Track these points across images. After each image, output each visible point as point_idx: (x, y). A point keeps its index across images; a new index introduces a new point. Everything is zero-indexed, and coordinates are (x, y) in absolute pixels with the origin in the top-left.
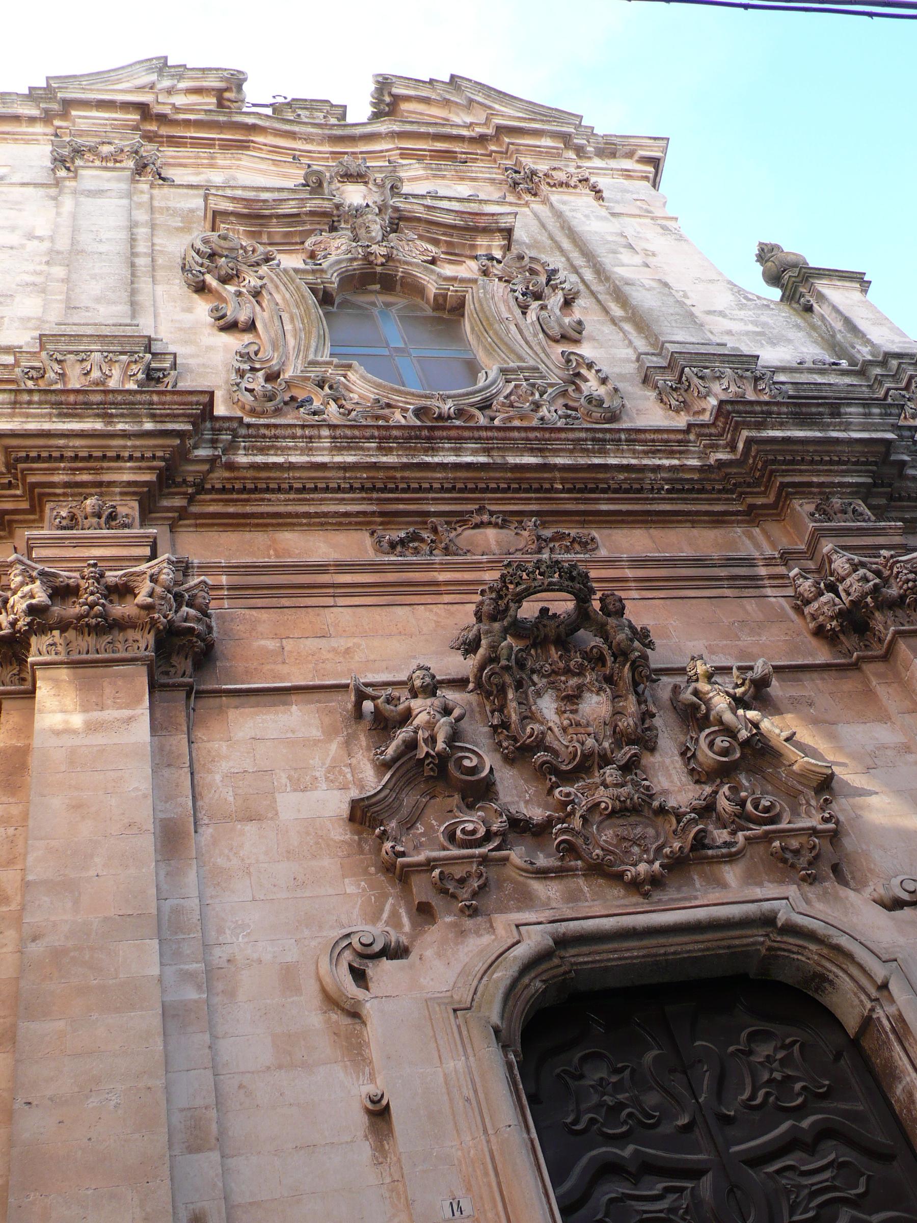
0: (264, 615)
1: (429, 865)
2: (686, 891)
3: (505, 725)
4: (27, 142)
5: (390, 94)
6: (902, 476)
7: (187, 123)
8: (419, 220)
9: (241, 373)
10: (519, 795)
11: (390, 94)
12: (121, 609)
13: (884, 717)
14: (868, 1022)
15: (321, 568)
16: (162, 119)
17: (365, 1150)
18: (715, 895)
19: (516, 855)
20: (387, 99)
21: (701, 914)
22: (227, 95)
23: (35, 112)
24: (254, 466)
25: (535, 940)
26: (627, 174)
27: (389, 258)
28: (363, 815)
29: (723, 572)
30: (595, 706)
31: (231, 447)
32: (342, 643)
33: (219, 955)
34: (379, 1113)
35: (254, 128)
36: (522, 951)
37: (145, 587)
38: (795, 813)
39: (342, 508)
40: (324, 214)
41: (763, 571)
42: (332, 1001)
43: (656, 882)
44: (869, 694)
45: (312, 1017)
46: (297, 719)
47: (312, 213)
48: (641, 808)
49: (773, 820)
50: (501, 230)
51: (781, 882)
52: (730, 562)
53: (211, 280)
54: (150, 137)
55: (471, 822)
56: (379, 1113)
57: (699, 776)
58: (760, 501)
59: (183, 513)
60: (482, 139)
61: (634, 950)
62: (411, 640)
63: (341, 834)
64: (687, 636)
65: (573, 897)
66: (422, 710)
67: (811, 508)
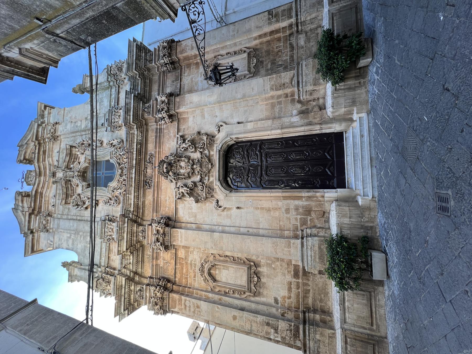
0: (162, 209)
2: (213, 160)
3: (185, 178)
4: (40, 237)
5: (23, 160)
6: (140, 94)
7: (35, 205)
8: (68, 164)
9: (110, 205)
10: (197, 178)
11: (23, 160)
12: (161, 231)
13: (188, 118)
14: (235, 141)
15: (154, 199)
16: (33, 210)
17: (241, 210)
18: (215, 156)
19: (206, 182)
20: (25, 161)
21: (217, 160)
22: (23, 195)
23: (31, 236)
24: (134, 208)
25: (218, 183)
26: (49, 113)
27: (79, 172)
28: (197, 201)
29: (158, 134)
30: (183, 164)
31: (130, 211)
32: (168, 198)
33: (215, 224)
34: (238, 208)
35: (36, 191)
36: (220, 186)
37: (158, 228)
38: (203, 140)
39: (142, 194)
40: (66, 182)
41: (159, 127)
42: (223, 211)
43: (212, 164)
44: (184, 119)
45: (225, 213)
46: (180, 206)
47: (66, 185)
48: (200, 163)
49: (204, 144)
50: (71, 148)
51: (214, 146)
52: (156, 132)
53: (84, 206)
54: (39, 212)
55: (200, 187)
56: (238, 208)
57: (195, 151)
58: (144, 123)
59: (142, 219)
60: (39, 144)
61: (221, 170)
62: (168, 190)
63: (199, 204)
64: (170, 145)
65: (213, 176)
66: (181, 190)
67: (147, 115)
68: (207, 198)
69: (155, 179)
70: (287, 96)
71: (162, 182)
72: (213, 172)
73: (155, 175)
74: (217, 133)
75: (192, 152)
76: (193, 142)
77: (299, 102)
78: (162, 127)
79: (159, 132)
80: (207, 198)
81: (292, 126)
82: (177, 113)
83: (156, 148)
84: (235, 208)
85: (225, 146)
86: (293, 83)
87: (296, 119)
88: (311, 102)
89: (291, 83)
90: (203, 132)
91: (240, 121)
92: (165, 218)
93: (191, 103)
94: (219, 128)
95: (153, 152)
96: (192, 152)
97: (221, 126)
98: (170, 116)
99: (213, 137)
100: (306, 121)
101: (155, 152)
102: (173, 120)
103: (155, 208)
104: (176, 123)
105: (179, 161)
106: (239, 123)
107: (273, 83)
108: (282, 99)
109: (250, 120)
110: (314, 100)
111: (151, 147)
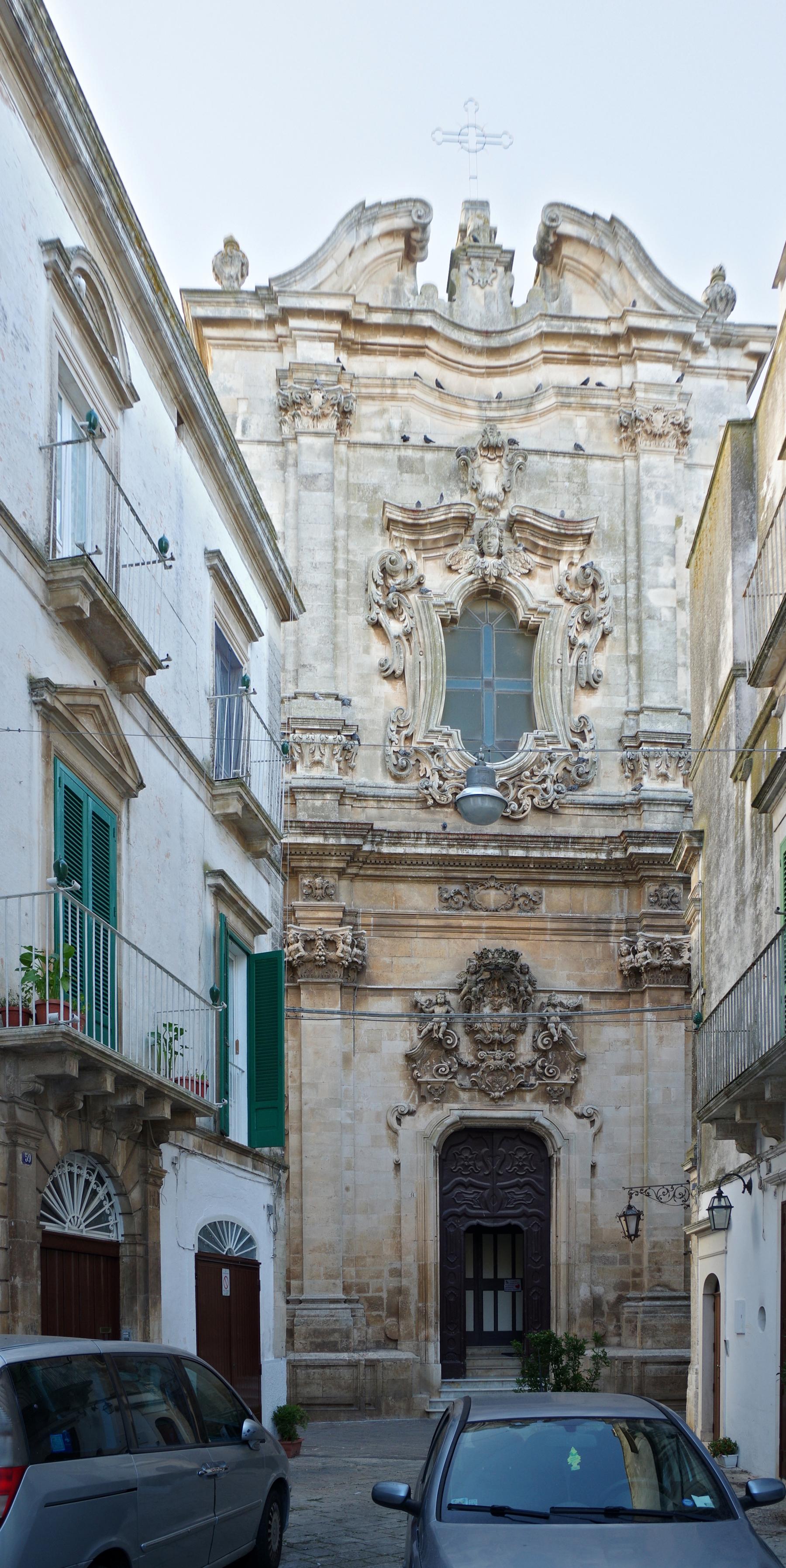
1: (428, 1083)
15: (413, 916)
17: (392, 1174)
34: (397, 1165)
42: (389, 1127)
43: (500, 1098)
45: (383, 1131)
46: (393, 1005)
51: (545, 1103)
56: (397, 1165)
57: (536, 1049)
63: (401, 1061)
65: (472, 1099)
68: (419, 1084)
69: (468, 917)
70: (637, 1274)
71: (459, 942)
72: (480, 1100)
73: (480, 918)
74: (575, 1109)
75: (535, 1041)
76: (562, 1044)
77: (620, 1299)
78: (612, 939)
79: (599, 928)
80: (419, 1084)
81: (571, 1284)
82: (643, 992)
83: (555, 919)
84: (395, 1157)
85: (542, 1133)
86: (659, 1288)
87: (584, 1292)
88: (614, 1322)
89: (658, 1285)
90: (585, 1069)
91: (599, 1169)
92: (364, 958)
93: (661, 1038)
94: (590, 1118)
95: (543, 907)
96: (535, 1041)
97: (593, 1123)
98: (635, 973)
99: (568, 1101)
100: (577, 1311)
101: (542, 919)
102: (625, 977)
103: (389, 921)
104: (616, 986)
105: (515, 1000)
106: (593, 1167)
107: (667, 1247)
108: (632, 1266)
109: (598, 1193)
110: (619, 1327)
111: (557, 899)
